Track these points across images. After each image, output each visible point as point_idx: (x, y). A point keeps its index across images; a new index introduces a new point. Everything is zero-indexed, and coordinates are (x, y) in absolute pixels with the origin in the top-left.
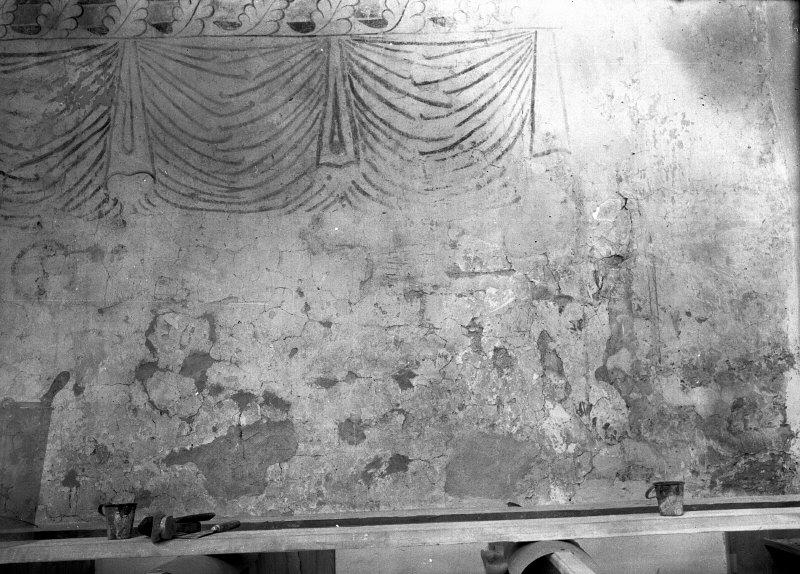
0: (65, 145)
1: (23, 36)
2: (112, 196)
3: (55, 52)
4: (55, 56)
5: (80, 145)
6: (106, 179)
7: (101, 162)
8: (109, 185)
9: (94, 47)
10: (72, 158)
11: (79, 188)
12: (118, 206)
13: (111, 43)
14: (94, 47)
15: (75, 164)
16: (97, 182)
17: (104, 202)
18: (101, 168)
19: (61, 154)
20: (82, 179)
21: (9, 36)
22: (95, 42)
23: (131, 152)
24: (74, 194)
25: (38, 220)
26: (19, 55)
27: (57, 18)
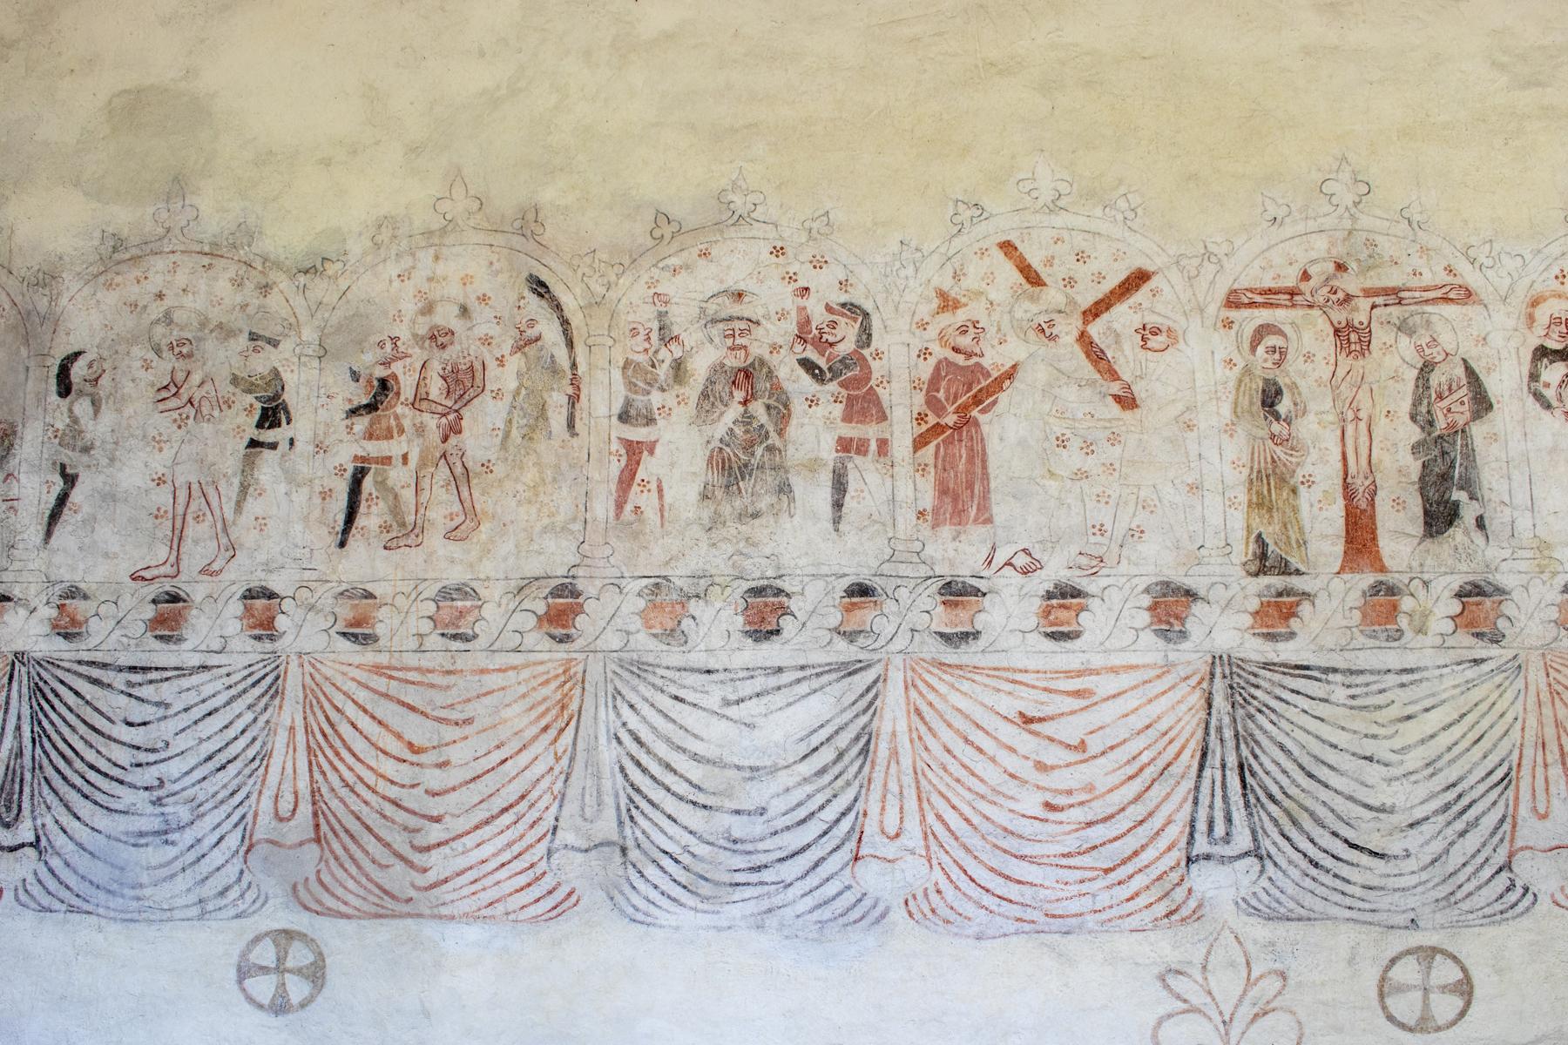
0: (1447, 807)
1: (1377, 643)
2: (1519, 883)
3: (1426, 668)
4: (1425, 674)
5: (1470, 806)
6: (1511, 855)
7: (1501, 831)
8: (1514, 866)
9: (1483, 661)
10: (1459, 825)
11: (1469, 869)
12: (1530, 897)
13: (1510, 654)
14: (1483, 661)
15: (1462, 834)
16: (1500, 858)
17: (1508, 890)
18: (1502, 840)
19: (1441, 819)
20: (1473, 856)
21: (1355, 644)
22: (1482, 654)
23: (1544, 817)
24: (1462, 877)
25: (1412, 915)
26: (1372, 672)
27: (1426, 615)
